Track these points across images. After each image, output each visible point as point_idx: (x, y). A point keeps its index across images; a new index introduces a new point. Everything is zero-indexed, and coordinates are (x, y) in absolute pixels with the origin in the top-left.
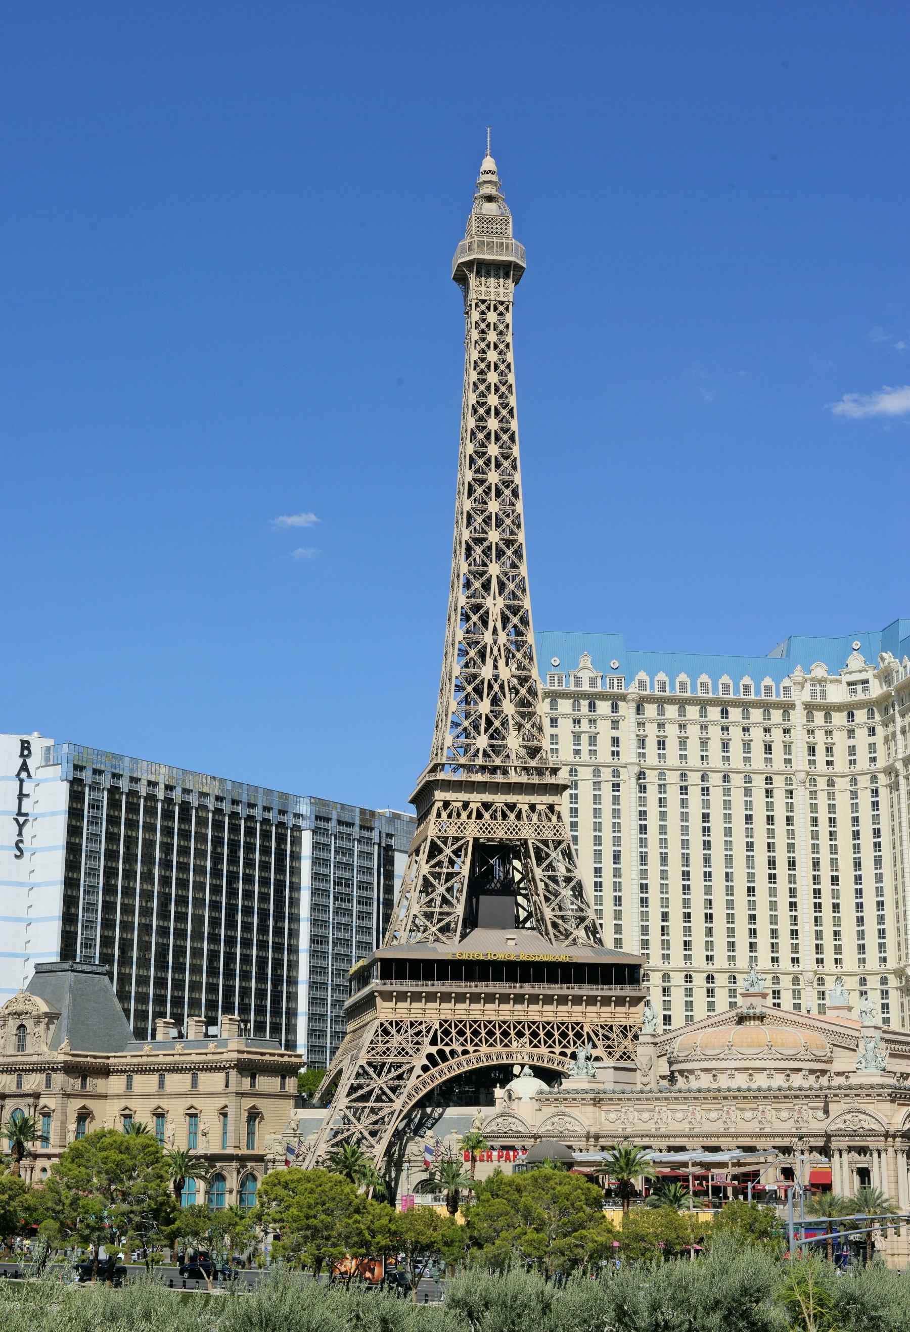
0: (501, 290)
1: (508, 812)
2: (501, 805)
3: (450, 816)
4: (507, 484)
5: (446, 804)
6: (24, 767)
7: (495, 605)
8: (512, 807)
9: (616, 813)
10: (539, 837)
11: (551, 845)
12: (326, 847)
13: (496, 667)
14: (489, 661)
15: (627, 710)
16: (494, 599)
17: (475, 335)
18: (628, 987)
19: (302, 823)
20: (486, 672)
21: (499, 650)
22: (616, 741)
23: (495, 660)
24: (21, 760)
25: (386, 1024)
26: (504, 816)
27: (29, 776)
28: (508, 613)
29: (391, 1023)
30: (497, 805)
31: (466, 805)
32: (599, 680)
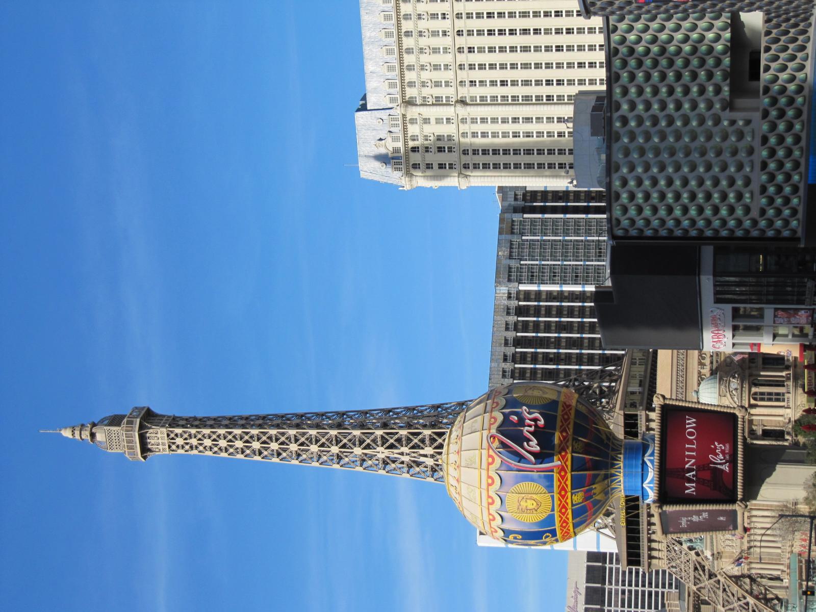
0: (159, 435)
4: (296, 440)
7: (382, 452)
9: (494, 120)
12: (530, 268)
13: (425, 456)
14: (422, 459)
15: (413, 112)
17: (195, 452)
18: (641, 527)
19: (513, 291)
21: (414, 452)
22: (439, 121)
25: (669, 566)
28: (387, 445)
29: (669, 563)
32: (394, 135)
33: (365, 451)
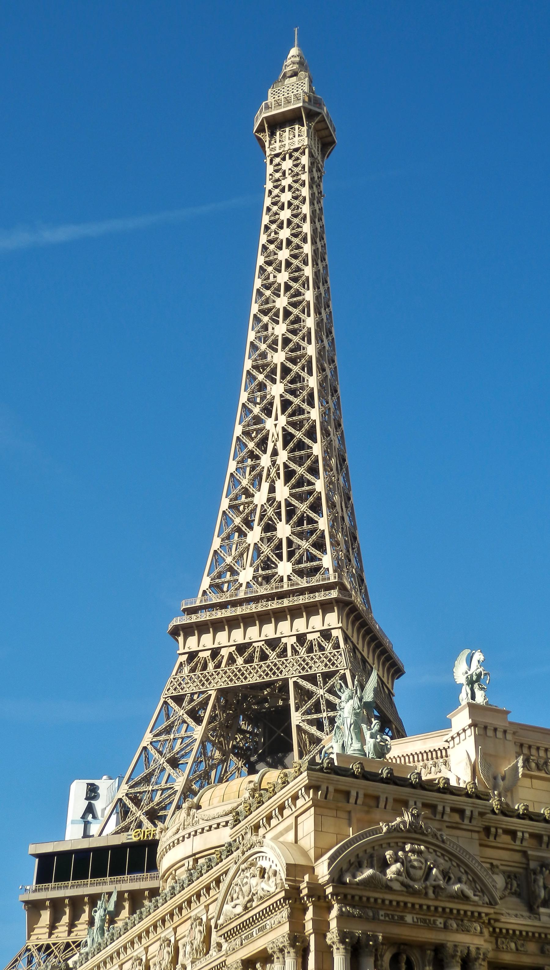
1: (268, 651)
2: (260, 644)
3: (193, 670)
5: (192, 655)
6: (90, 809)
7: (276, 425)
8: (273, 643)
10: (304, 673)
11: (320, 680)
13: (272, 489)
14: (265, 486)
16: (276, 419)
20: (260, 498)
23: (273, 481)
24: (87, 802)
26: (264, 657)
27: (94, 817)
29: (39, 949)
30: (255, 645)
31: (215, 653)
33: (277, 403)
